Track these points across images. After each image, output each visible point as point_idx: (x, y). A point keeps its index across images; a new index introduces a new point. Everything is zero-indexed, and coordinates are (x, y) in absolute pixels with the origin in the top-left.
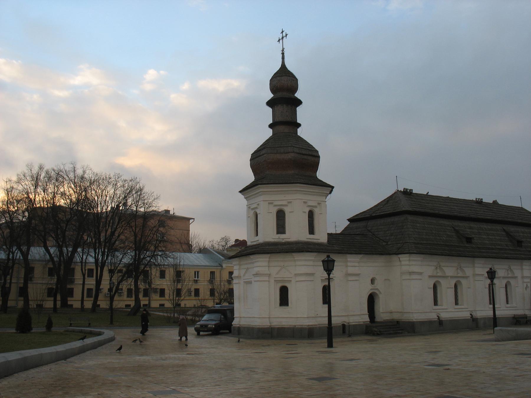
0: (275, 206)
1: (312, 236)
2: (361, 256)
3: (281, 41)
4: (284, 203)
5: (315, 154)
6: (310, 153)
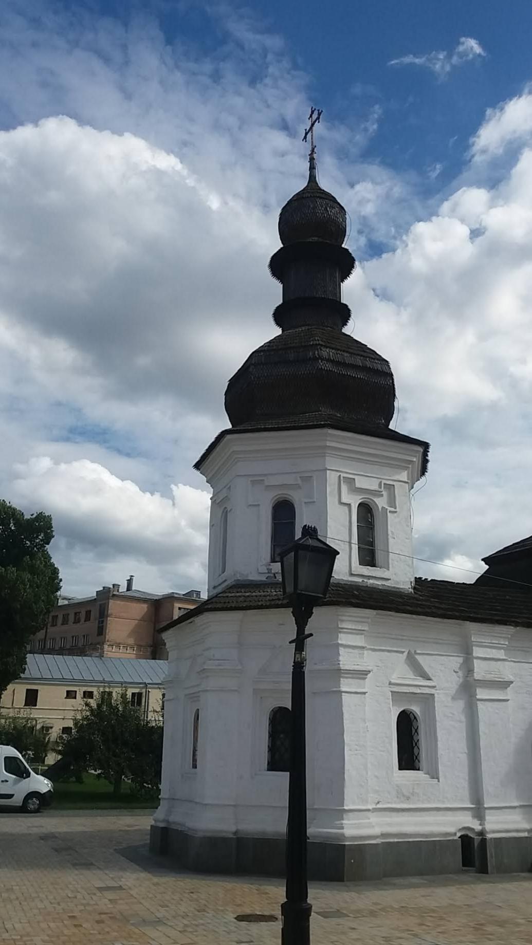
0: (268, 487)
1: (367, 570)
2: (511, 629)
3: (309, 136)
4: (289, 480)
5: (385, 369)
6: (368, 364)
